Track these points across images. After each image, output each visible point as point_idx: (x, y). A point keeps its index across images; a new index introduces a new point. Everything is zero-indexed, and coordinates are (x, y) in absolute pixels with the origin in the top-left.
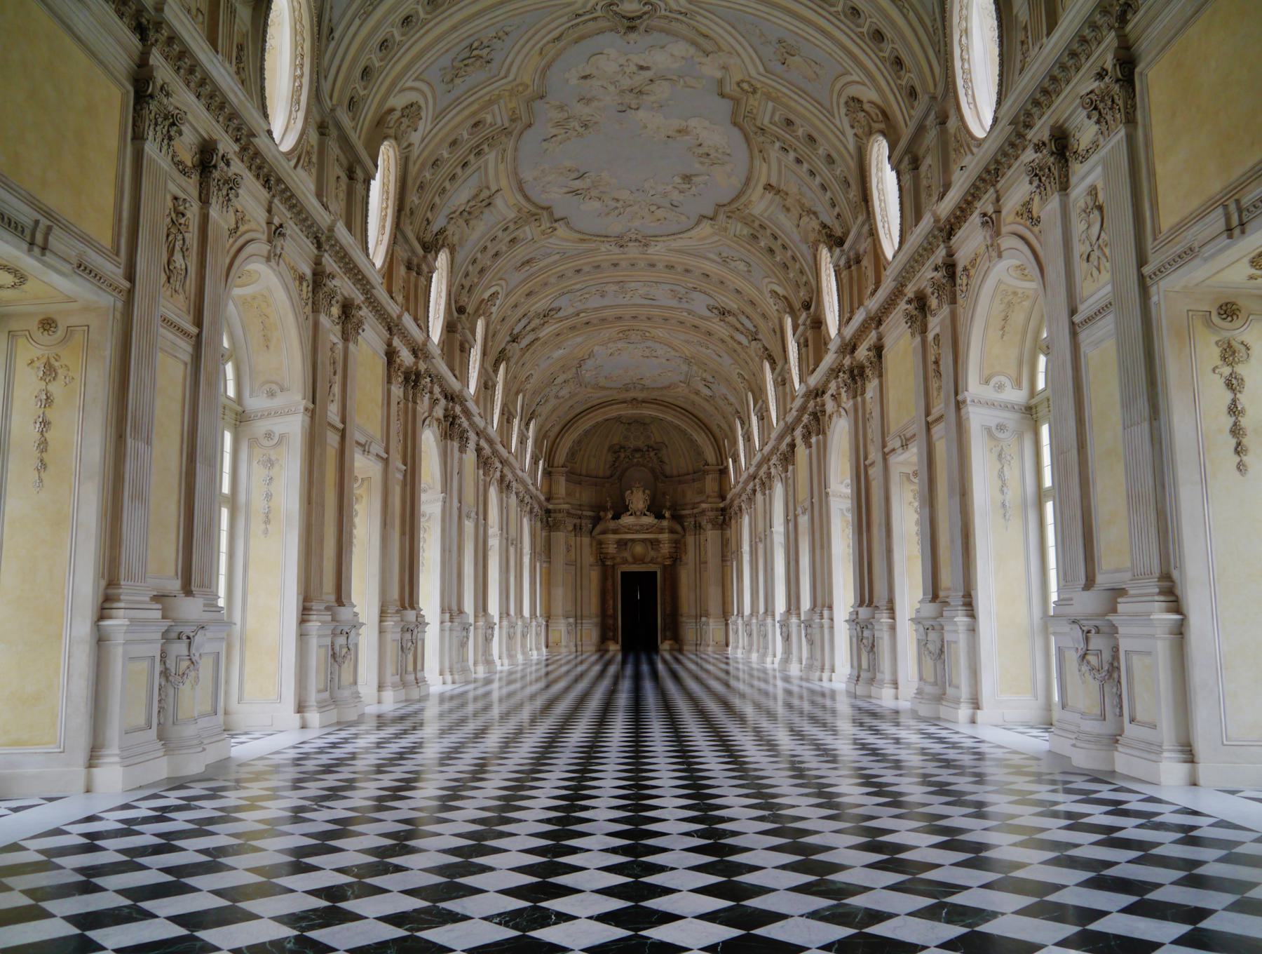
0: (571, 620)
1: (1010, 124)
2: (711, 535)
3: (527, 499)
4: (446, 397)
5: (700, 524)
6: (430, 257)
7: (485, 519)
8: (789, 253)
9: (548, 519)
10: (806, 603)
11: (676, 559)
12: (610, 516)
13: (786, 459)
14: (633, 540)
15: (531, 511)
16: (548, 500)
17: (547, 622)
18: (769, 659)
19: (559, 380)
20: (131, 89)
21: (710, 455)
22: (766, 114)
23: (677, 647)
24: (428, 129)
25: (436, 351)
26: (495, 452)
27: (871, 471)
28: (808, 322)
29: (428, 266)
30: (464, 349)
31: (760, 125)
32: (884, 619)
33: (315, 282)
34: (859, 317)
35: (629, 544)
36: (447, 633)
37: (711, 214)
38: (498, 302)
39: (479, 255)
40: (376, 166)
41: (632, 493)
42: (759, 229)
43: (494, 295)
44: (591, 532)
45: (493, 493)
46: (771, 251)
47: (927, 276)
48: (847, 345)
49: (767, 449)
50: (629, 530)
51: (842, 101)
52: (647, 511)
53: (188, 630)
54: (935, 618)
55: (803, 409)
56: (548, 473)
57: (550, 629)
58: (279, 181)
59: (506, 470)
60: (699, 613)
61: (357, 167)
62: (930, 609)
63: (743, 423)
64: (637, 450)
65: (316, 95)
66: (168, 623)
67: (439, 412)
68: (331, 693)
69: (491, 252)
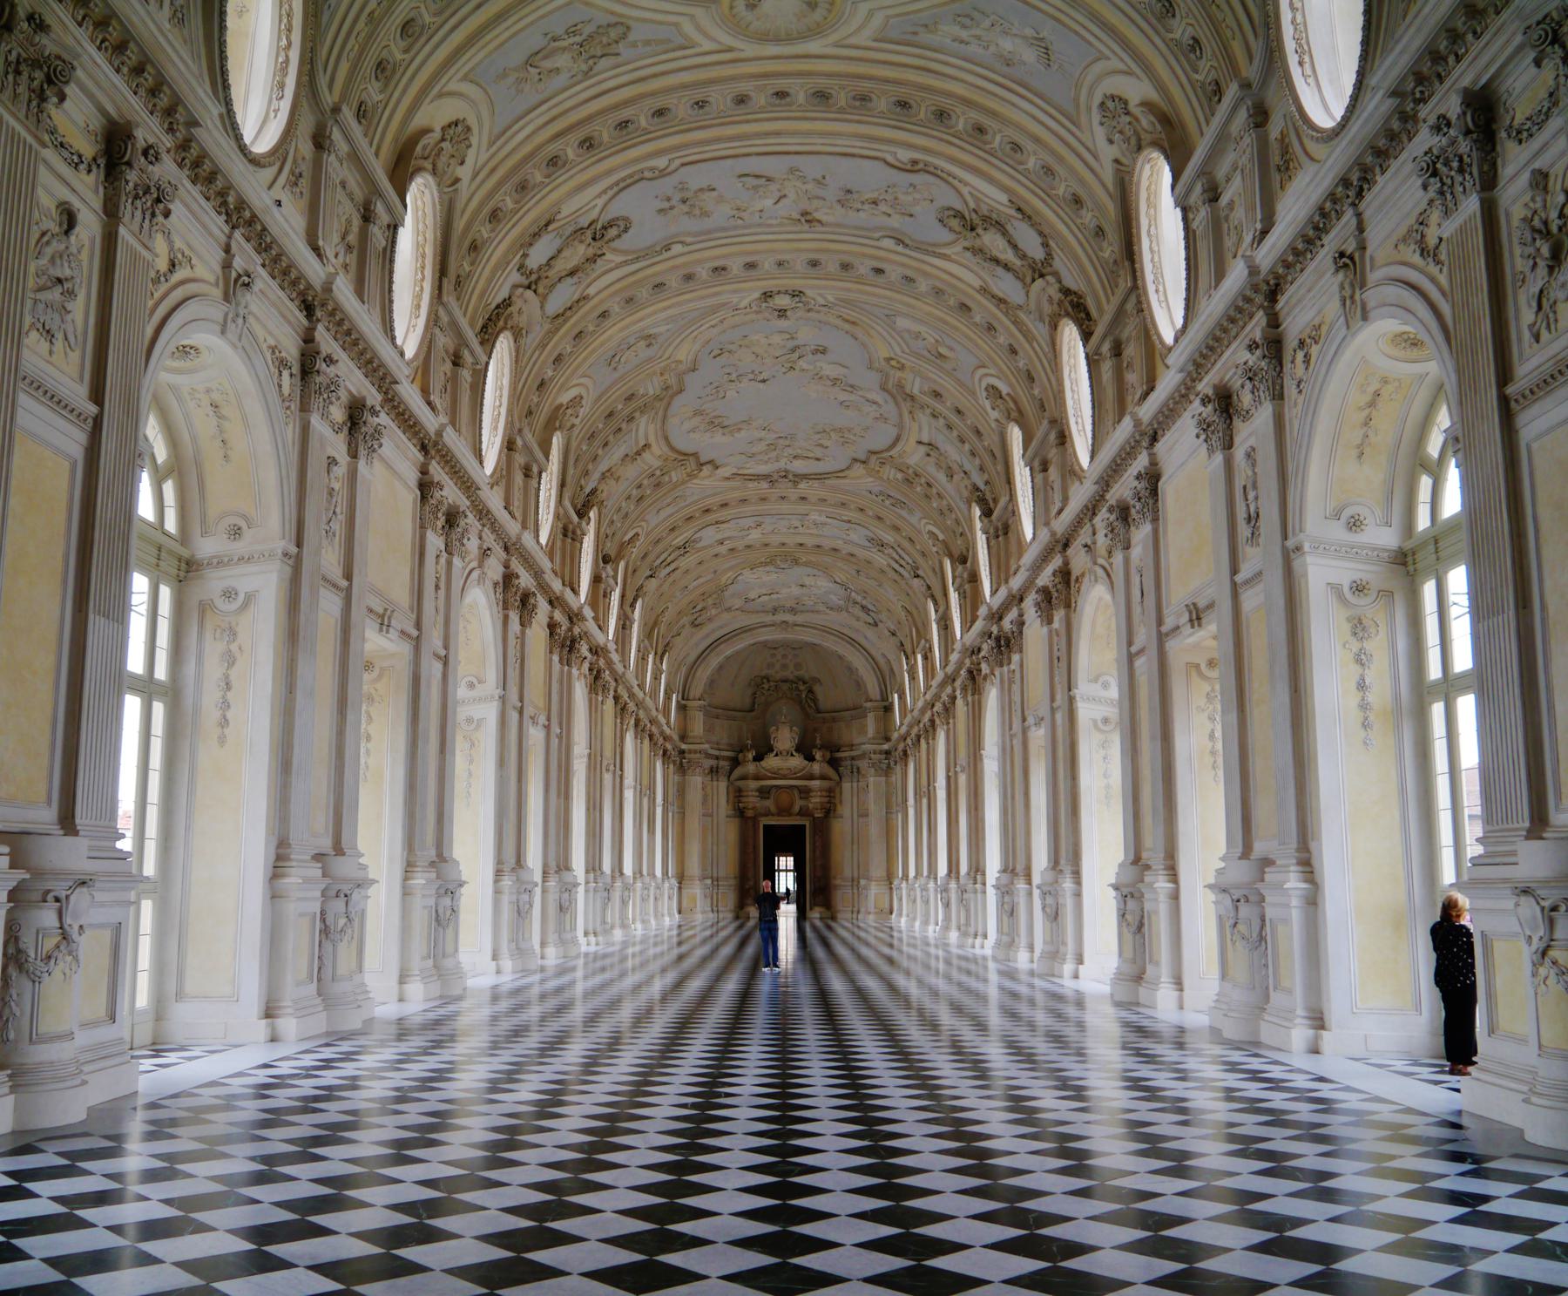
0: (709, 882)
1: (1095, 483)
2: (873, 780)
3: (661, 741)
4: (591, 650)
7: (621, 770)
8: (945, 502)
9: (679, 761)
10: (964, 868)
11: (829, 810)
12: (750, 756)
13: (946, 710)
14: (776, 786)
15: (664, 754)
16: (683, 738)
17: (680, 883)
18: (931, 928)
19: (699, 608)
20: (419, 493)
21: (872, 686)
22: (915, 387)
23: (828, 914)
25: (588, 613)
26: (632, 695)
27: (1015, 742)
28: (965, 575)
29: (581, 530)
30: (607, 595)
31: (908, 391)
32: (1021, 886)
34: (1003, 593)
35: (774, 791)
36: (591, 894)
37: (863, 457)
38: (638, 544)
43: (637, 534)
46: (927, 496)
47: (1045, 578)
49: (928, 697)
50: (777, 775)
51: (984, 385)
52: (796, 750)
53: (345, 888)
54: (1051, 884)
55: (960, 664)
56: (682, 708)
57: (684, 891)
58: (488, 511)
59: (642, 714)
60: (856, 875)
61: (466, 352)
62: (1005, 878)
63: (907, 658)
64: (785, 681)
65: (510, 424)
66: (328, 880)
67: (586, 665)
68: (435, 961)
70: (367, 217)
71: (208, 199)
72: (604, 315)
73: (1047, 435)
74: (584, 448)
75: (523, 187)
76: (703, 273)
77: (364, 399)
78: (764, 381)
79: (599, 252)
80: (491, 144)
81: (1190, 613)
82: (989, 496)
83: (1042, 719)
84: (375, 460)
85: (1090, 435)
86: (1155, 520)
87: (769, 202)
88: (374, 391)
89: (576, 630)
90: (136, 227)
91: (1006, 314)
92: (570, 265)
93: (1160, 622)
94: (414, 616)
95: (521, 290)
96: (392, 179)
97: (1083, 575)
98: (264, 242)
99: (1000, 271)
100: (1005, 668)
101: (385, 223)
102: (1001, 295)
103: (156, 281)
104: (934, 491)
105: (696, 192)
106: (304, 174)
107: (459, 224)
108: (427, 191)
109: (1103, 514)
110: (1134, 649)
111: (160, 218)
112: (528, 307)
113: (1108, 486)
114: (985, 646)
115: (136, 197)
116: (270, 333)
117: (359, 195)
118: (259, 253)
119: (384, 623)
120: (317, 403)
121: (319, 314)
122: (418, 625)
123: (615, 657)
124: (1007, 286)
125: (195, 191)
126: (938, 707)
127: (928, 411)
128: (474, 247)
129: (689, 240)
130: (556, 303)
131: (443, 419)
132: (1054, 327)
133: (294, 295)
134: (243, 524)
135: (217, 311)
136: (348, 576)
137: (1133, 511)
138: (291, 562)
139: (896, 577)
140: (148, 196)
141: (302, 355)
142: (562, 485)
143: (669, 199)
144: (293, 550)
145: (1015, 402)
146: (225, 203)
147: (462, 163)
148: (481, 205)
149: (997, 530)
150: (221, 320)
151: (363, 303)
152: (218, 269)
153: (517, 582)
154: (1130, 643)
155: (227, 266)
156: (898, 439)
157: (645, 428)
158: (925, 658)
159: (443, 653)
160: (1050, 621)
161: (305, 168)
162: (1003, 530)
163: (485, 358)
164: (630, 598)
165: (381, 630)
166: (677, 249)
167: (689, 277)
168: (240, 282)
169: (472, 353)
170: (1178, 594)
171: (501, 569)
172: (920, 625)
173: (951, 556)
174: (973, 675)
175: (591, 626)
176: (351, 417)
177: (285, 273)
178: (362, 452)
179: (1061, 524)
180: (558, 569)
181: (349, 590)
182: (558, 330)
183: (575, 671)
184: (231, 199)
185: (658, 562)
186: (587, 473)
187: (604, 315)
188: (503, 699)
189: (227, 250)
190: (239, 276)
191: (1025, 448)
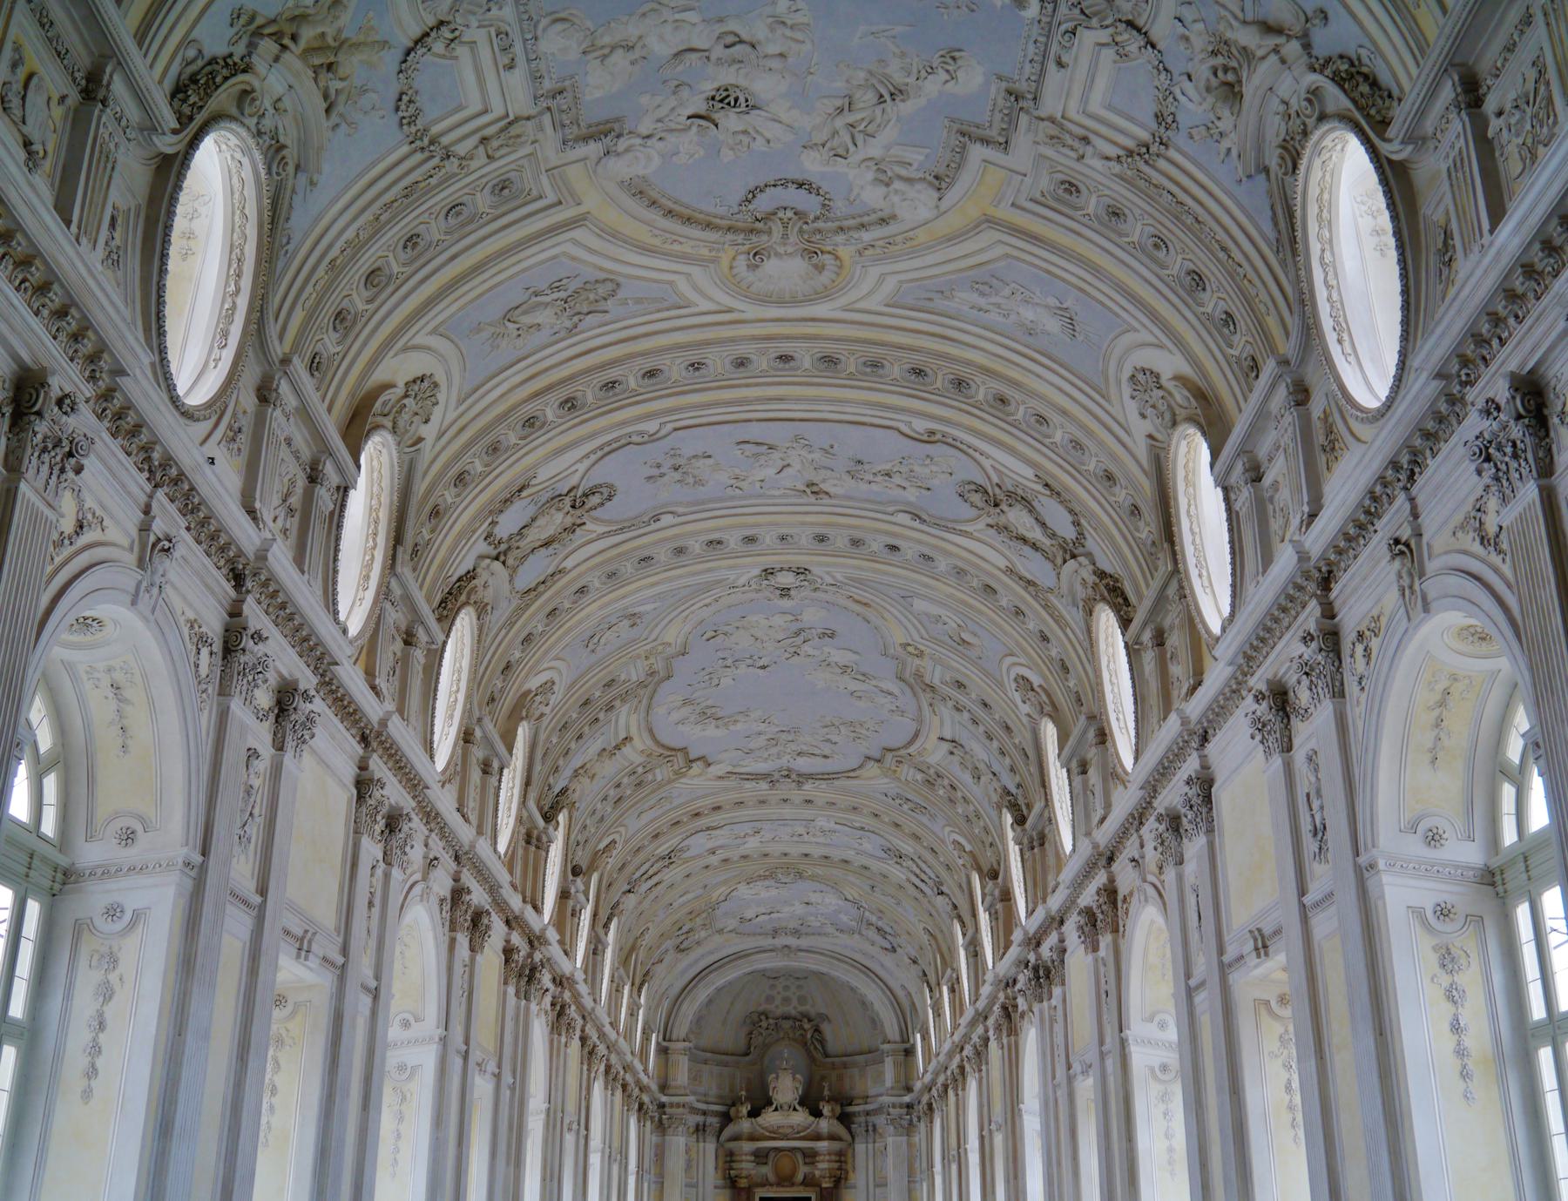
3: (636, 1092)
4: (554, 980)
5: (874, 1126)
6: (551, 829)
7: (587, 1128)
9: (658, 1117)
12: (744, 1110)
13: (978, 1054)
16: (664, 1087)
19: (685, 929)
20: (355, 792)
21: (891, 1029)
22: (936, 676)
24: (560, 697)
26: (602, 1036)
27: (1059, 1093)
28: (997, 892)
30: (575, 913)
31: (928, 682)
33: (452, 899)
34: (1040, 914)
35: (772, 1154)
37: (877, 755)
38: (615, 853)
39: (599, 806)
40: (511, 754)
41: (777, 1078)
42: (935, 777)
43: (614, 842)
44: (718, 1137)
45: (598, 1088)
46: (951, 800)
47: (1088, 897)
48: (1030, 939)
49: (956, 1038)
50: (775, 1134)
51: (1013, 676)
52: (800, 1104)
55: (992, 999)
56: (663, 1051)
58: (437, 814)
59: (614, 1059)
63: (931, 990)
64: (786, 1018)
65: (468, 712)
67: (548, 999)
69: (611, 800)
70: (314, 477)
71: (129, 454)
72: (582, 591)
73: (1085, 732)
74: (554, 741)
75: (494, 449)
76: (696, 546)
77: (296, 682)
78: (763, 667)
79: (579, 521)
80: (460, 402)
81: (1255, 940)
82: (1021, 801)
83: (1090, 1066)
84: (304, 754)
85: (1133, 733)
86: (1210, 831)
87: (772, 471)
88: (308, 672)
89: (537, 957)
90: (40, 484)
91: (1035, 597)
92: (544, 536)
93: (1221, 951)
94: (340, 940)
95: (488, 561)
96: (344, 437)
97: (1131, 894)
98: (190, 503)
99: (1027, 550)
100: (1045, 1003)
101: (335, 485)
102: (1029, 577)
103: (59, 544)
104: (959, 794)
105: (689, 459)
106: (244, 429)
107: (420, 488)
108: (384, 451)
109: (1151, 824)
110: (1192, 983)
111: (70, 474)
112: (495, 580)
113: (1155, 791)
114: (1022, 979)
115: (44, 450)
116: (190, 605)
117: (306, 455)
118: (184, 515)
119: (303, 947)
120: (239, 686)
121: (249, 584)
122: (345, 950)
123: (583, 989)
124: (1035, 567)
125: (115, 445)
126: (968, 1051)
127: (950, 704)
128: (436, 513)
129: (680, 510)
130: (529, 575)
131: (390, 706)
132: (1090, 613)
133: (222, 562)
134: (139, 828)
135: (129, 578)
136: (263, 891)
137: (1184, 820)
138: (193, 873)
139: (920, 896)
140: (58, 450)
141: (226, 631)
142: (527, 783)
143: (659, 466)
144: (197, 858)
145: (1049, 696)
146: (148, 459)
147: (426, 422)
148: (447, 466)
149: (1031, 841)
150: (132, 590)
151: (303, 572)
152: (134, 533)
153: (468, 898)
154: (1188, 976)
155: (145, 528)
156: (916, 735)
157: (626, 719)
158: (952, 990)
159: (373, 984)
160: (1095, 949)
161: (246, 422)
162: (1039, 842)
163: (443, 637)
164: (603, 916)
165: (298, 956)
166: (667, 520)
167: (680, 551)
168: (159, 547)
169: (428, 631)
170: (1242, 914)
171: (449, 883)
172: (945, 950)
173: (979, 870)
174: (1008, 1012)
175: (555, 951)
176: (279, 702)
177: (213, 537)
178: (290, 743)
179: (1104, 835)
180: (518, 882)
181: (262, 908)
182: (528, 606)
183: (534, 1007)
184: (156, 455)
185: (638, 874)
186: (557, 770)
187: (582, 591)
188: (444, 1041)
189: (147, 511)
190: (159, 540)
191: (1061, 748)
